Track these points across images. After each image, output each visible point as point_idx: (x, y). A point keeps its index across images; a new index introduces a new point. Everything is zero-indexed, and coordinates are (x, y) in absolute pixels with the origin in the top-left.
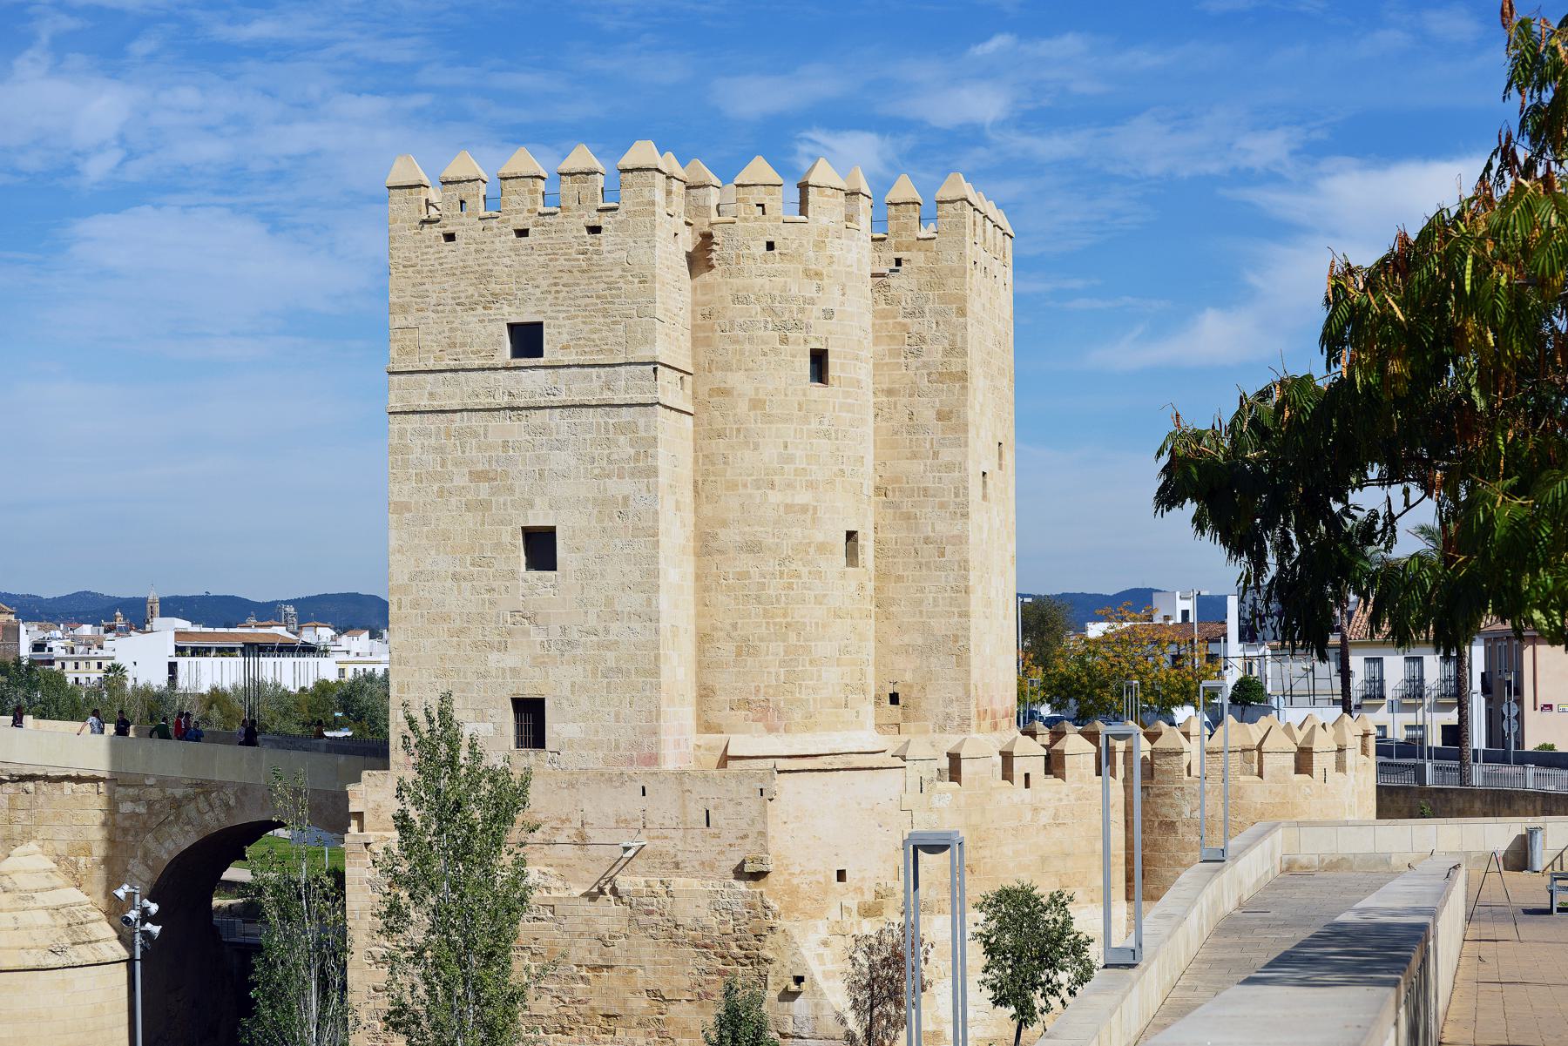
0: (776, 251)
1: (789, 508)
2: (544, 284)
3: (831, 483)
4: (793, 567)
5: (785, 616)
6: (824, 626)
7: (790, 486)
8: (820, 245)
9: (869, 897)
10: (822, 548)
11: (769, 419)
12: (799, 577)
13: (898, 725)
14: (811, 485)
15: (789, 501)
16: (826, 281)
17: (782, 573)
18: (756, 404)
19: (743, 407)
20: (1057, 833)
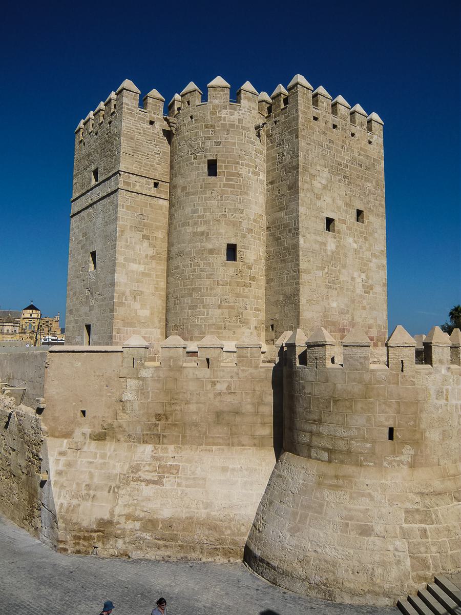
0: (193, 119)
1: (195, 234)
2: (99, 151)
3: (219, 221)
4: (196, 261)
5: (192, 285)
6: (211, 289)
7: (196, 223)
8: (213, 113)
9: (99, 430)
10: (211, 251)
11: (188, 194)
12: (199, 266)
13: (273, 340)
14: (205, 222)
15: (195, 231)
16: (216, 128)
17: (191, 264)
18: (184, 189)
19: (180, 190)
20: (229, 399)
